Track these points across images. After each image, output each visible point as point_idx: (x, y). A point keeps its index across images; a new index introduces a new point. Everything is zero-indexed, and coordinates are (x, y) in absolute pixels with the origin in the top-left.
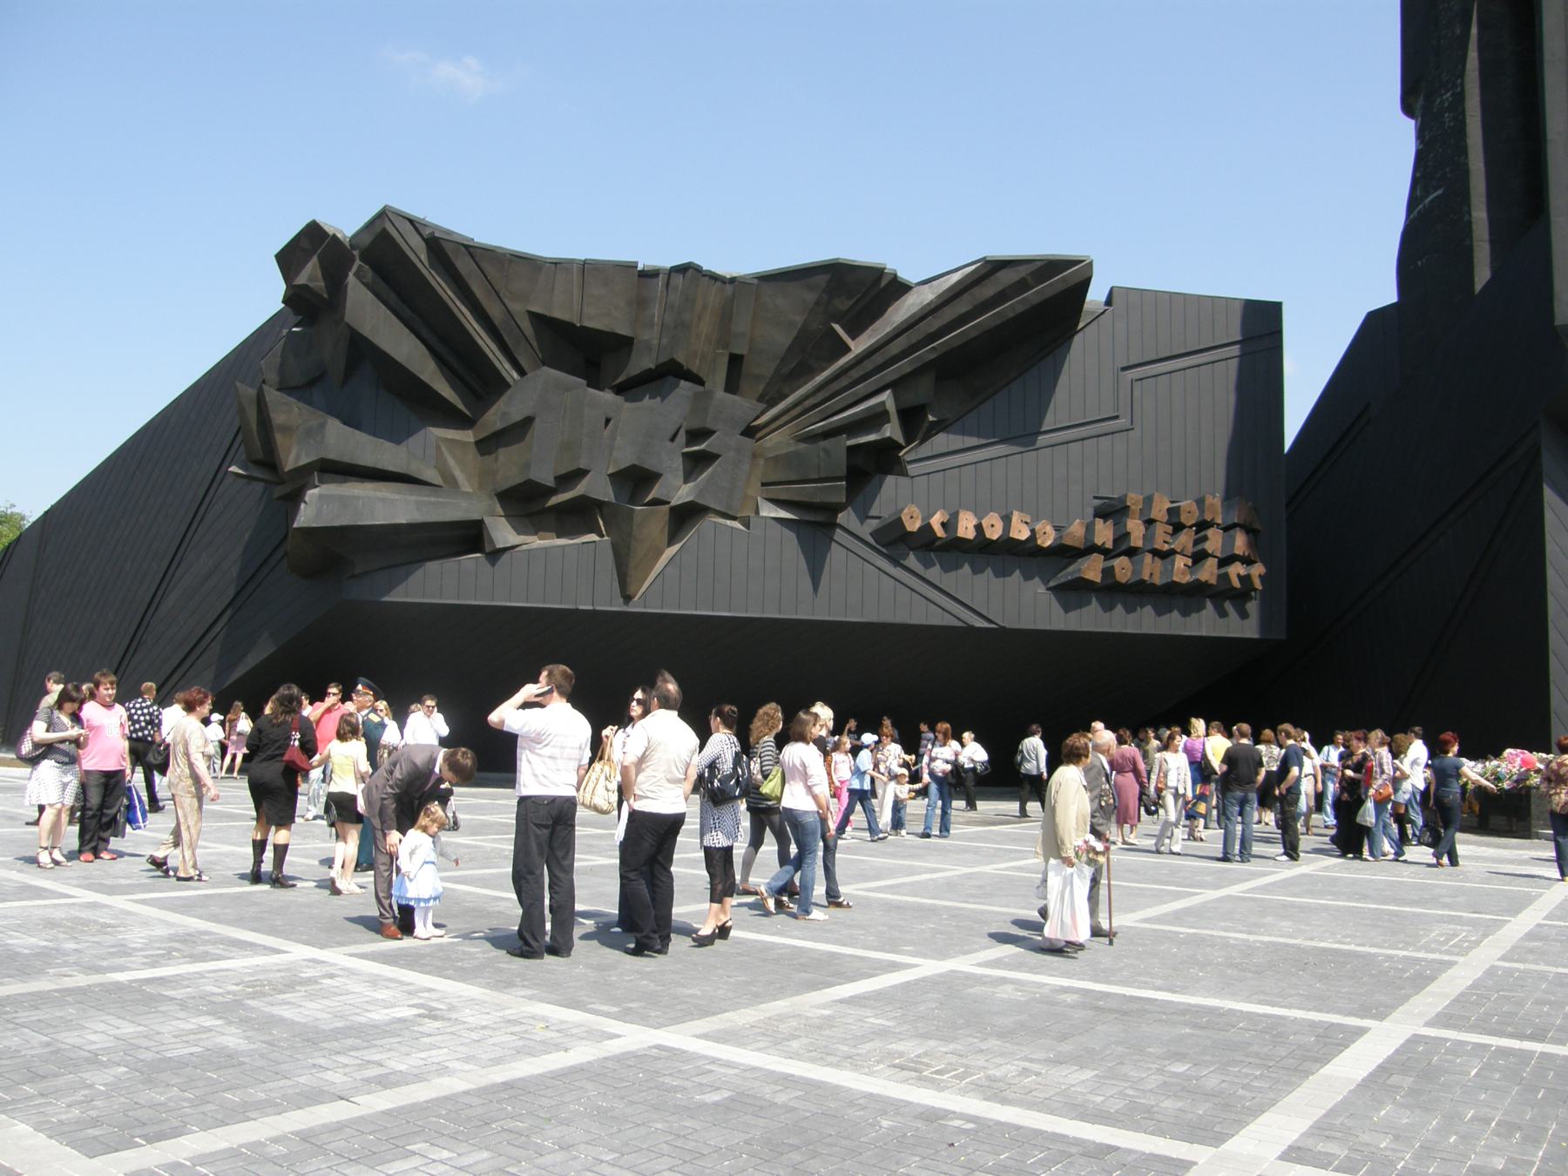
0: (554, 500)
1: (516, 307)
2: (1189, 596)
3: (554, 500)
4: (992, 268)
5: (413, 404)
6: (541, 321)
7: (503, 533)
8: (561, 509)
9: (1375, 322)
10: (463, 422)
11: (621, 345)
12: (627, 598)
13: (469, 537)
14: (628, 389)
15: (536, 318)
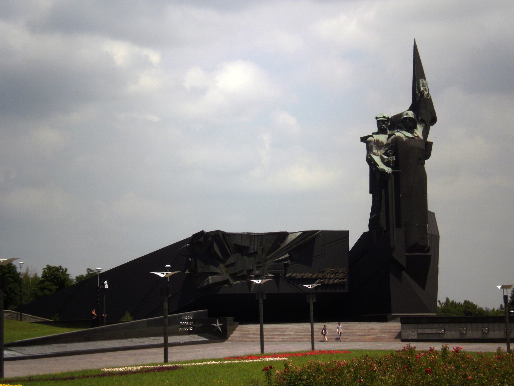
0: (238, 275)
1: (232, 243)
2: (334, 286)
3: (238, 275)
4: (305, 233)
5: (214, 260)
6: (235, 245)
7: (231, 281)
8: (239, 276)
9: (365, 234)
10: (223, 262)
11: (247, 248)
12: (250, 291)
13: (227, 282)
14: (250, 255)
15: (234, 244)
